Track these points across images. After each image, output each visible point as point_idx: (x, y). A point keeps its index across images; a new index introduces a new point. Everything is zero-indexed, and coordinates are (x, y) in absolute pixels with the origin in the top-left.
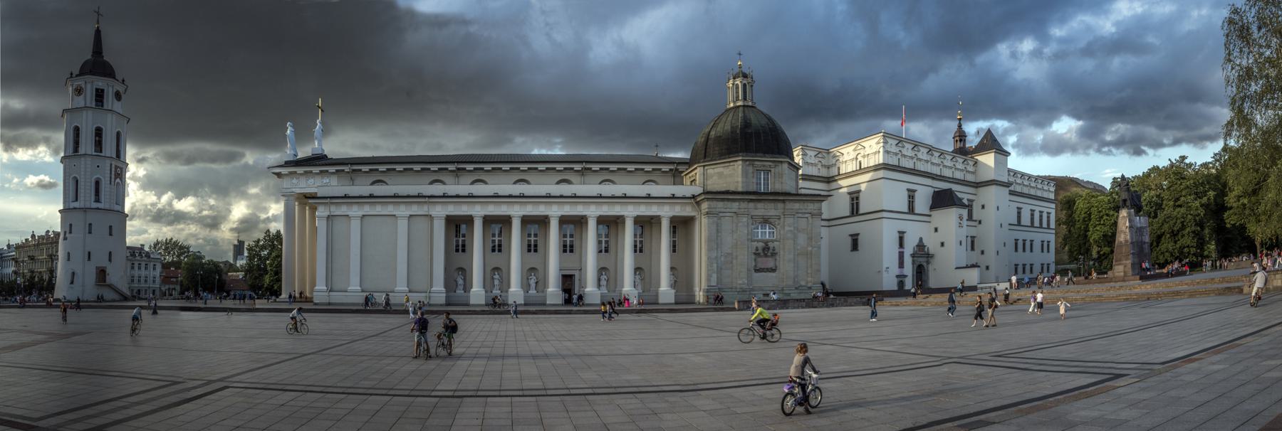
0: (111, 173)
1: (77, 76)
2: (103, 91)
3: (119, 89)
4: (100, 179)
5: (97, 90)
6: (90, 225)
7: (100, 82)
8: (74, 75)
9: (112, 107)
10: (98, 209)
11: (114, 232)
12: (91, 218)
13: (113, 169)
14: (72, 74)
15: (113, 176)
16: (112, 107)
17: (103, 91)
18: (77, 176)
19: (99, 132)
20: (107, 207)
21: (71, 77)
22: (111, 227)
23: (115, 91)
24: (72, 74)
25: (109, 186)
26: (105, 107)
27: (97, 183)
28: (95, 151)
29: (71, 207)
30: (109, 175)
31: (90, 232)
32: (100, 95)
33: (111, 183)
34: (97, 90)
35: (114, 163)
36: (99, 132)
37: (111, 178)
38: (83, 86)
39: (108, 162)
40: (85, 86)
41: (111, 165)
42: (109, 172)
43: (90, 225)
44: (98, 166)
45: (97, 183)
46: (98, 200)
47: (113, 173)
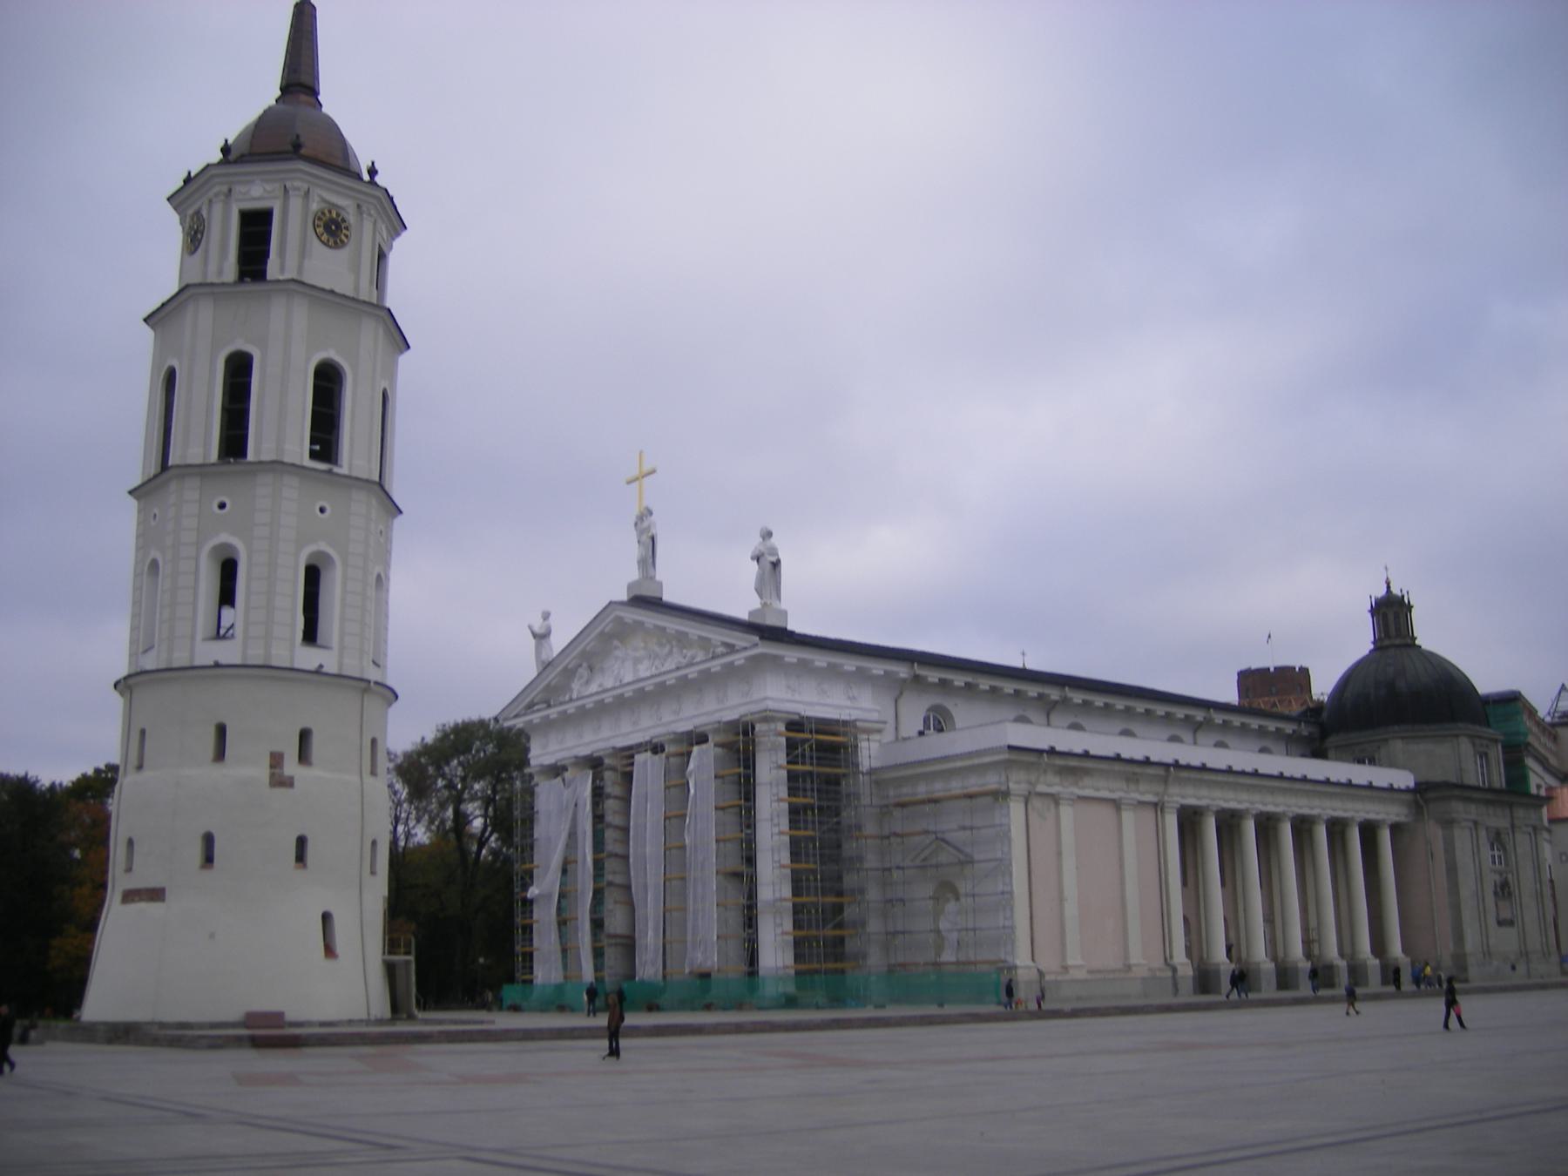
4: (226, 546)
9: (300, 269)
16: (300, 269)
19: (239, 370)
20: (256, 655)
23: (315, 206)
26: (273, 270)
36: (239, 370)
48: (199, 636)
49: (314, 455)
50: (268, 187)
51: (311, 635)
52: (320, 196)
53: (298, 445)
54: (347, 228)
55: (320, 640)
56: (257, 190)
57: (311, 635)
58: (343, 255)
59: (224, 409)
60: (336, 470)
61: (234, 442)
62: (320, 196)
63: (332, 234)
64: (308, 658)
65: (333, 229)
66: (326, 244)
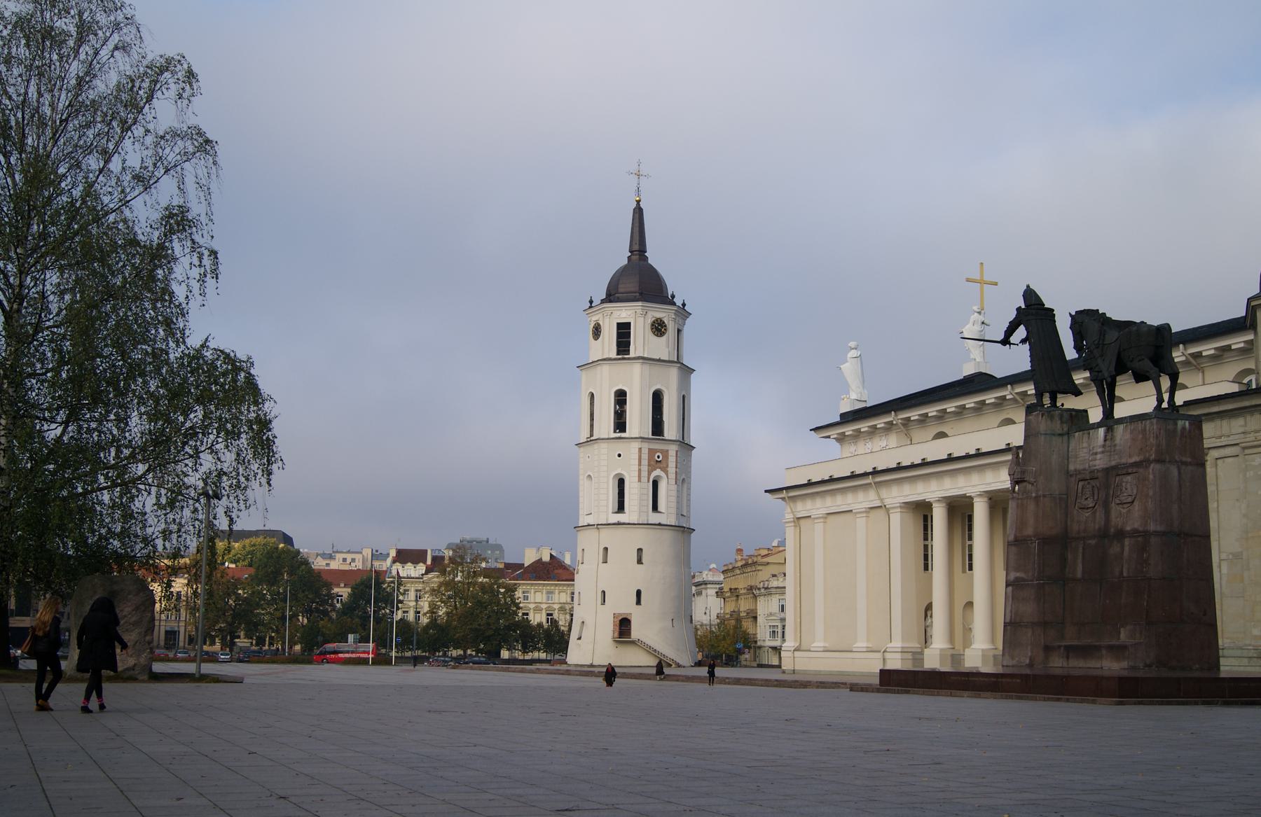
0: (640, 464)
1: (603, 301)
2: (627, 325)
3: (659, 315)
5: (618, 324)
6: (606, 549)
7: (635, 314)
8: (596, 301)
10: (619, 524)
11: (644, 560)
12: (607, 537)
13: (645, 456)
14: (591, 302)
15: (645, 468)
17: (627, 325)
19: (621, 397)
21: (591, 307)
22: (640, 550)
23: (649, 321)
24: (591, 302)
25: (636, 485)
26: (632, 354)
27: (621, 482)
28: (615, 432)
29: (611, 521)
30: (636, 468)
32: (624, 331)
35: (646, 447)
36: (621, 397)
37: (640, 470)
38: (601, 324)
39: (635, 446)
40: (603, 322)
42: (637, 462)
43: (606, 549)
44: (619, 455)
45: (621, 482)
46: (621, 508)
47: (645, 462)
48: (611, 511)
50: (629, 313)
51: (655, 508)
53: (648, 431)
55: (659, 510)
57: (655, 508)
58: (664, 338)
59: (614, 423)
61: (620, 425)
63: (657, 329)
64: (655, 518)
66: (657, 335)
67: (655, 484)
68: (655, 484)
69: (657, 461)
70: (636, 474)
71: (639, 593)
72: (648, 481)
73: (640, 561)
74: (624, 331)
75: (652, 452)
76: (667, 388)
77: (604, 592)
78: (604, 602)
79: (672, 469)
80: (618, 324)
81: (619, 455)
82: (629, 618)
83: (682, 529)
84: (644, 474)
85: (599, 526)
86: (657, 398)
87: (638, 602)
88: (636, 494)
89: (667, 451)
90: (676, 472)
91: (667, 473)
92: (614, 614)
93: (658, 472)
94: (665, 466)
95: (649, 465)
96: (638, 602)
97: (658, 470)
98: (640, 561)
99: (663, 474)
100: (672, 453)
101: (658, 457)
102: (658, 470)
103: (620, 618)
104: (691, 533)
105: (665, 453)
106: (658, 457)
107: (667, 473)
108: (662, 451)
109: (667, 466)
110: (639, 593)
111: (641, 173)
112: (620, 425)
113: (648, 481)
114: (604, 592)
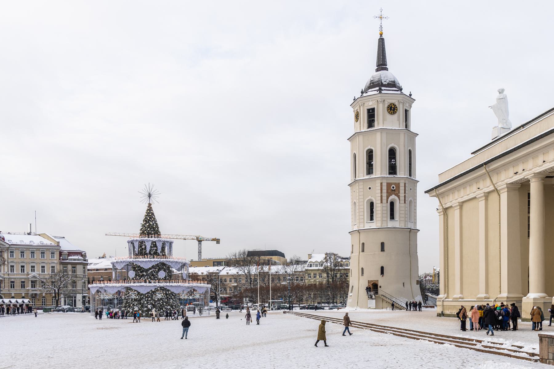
0: (381, 192)
2: (373, 110)
5: (369, 110)
6: (363, 244)
13: (385, 188)
15: (385, 195)
17: (373, 110)
18: (355, 201)
19: (370, 154)
27: (372, 204)
30: (380, 195)
31: (363, 251)
32: (371, 113)
33: (382, 202)
34: (369, 110)
36: (370, 154)
37: (381, 196)
38: (359, 111)
41: (381, 184)
43: (363, 244)
44: (370, 188)
45: (372, 204)
47: (385, 191)
49: (390, 173)
50: (374, 102)
52: (387, 102)
54: (396, 110)
56: (371, 103)
57: (392, 217)
60: (396, 176)
62: (387, 102)
64: (391, 224)
65: (392, 109)
67: (392, 204)
68: (392, 204)
69: (392, 190)
70: (380, 198)
71: (382, 268)
72: (387, 202)
73: (383, 249)
74: (371, 113)
75: (389, 185)
76: (399, 146)
77: (362, 269)
78: (363, 273)
79: (402, 194)
80: (367, 109)
81: (370, 188)
82: (377, 283)
83: (410, 230)
84: (385, 198)
85: (359, 231)
86: (392, 153)
87: (382, 272)
88: (381, 209)
89: (399, 183)
90: (405, 196)
91: (399, 197)
92: (368, 281)
93: (393, 197)
94: (397, 193)
95: (387, 192)
96: (382, 272)
97: (393, 195)
98: (383, 249)
99: (396, 198)
100: (402, 185)
101: (393, 187)
102: (393, 195)
103: (372, 283)
104: (417, 233)
105: (398, 185)
106: (393, 187)
107: (399, 197)
108: (395, 184)
109: (399, 192)
110: (382, 268)
111: (382, 17)
112: (370, 169)
113: (387, 202)
114: (362, 269)
